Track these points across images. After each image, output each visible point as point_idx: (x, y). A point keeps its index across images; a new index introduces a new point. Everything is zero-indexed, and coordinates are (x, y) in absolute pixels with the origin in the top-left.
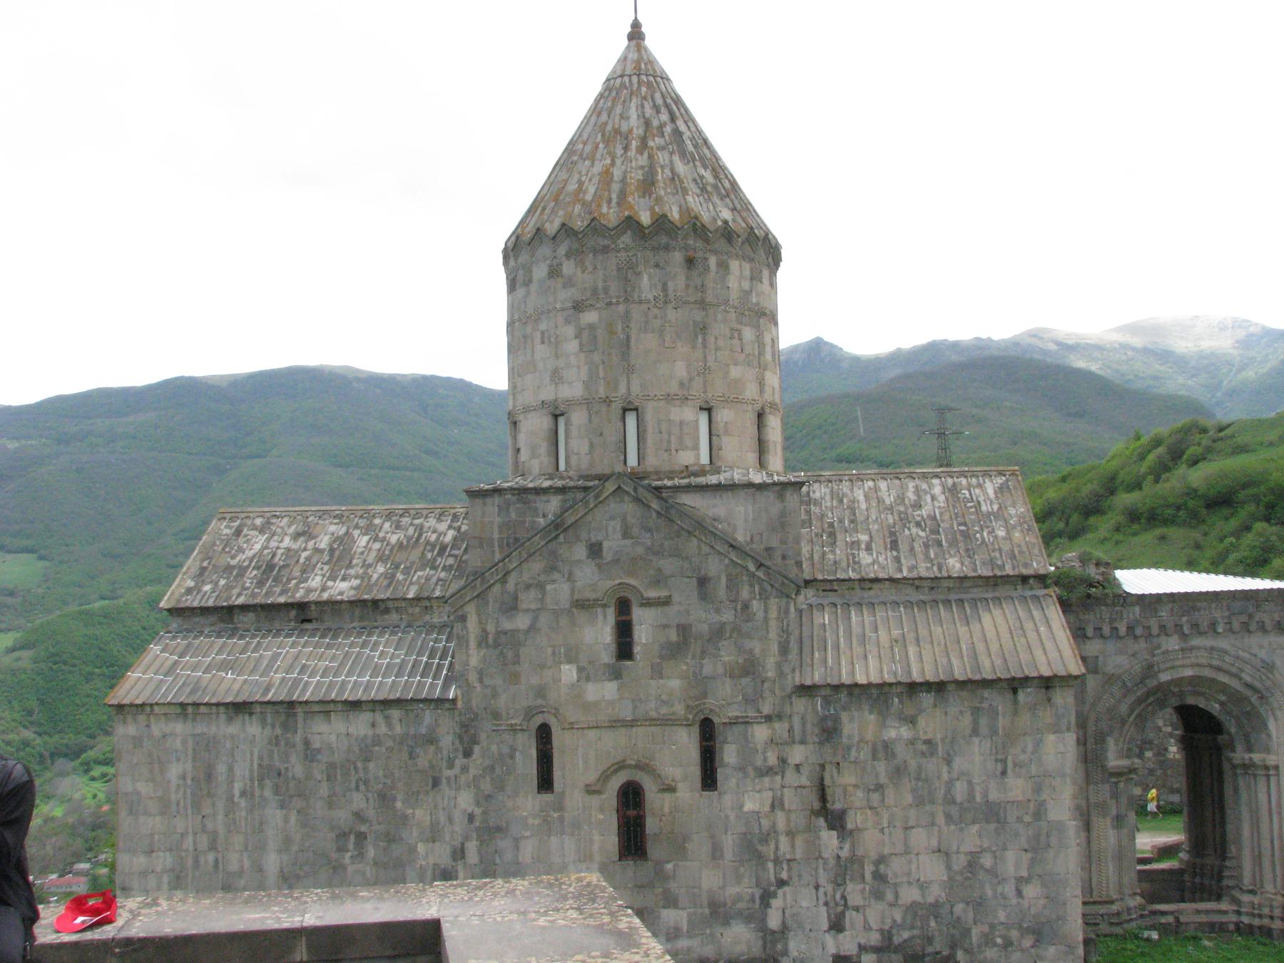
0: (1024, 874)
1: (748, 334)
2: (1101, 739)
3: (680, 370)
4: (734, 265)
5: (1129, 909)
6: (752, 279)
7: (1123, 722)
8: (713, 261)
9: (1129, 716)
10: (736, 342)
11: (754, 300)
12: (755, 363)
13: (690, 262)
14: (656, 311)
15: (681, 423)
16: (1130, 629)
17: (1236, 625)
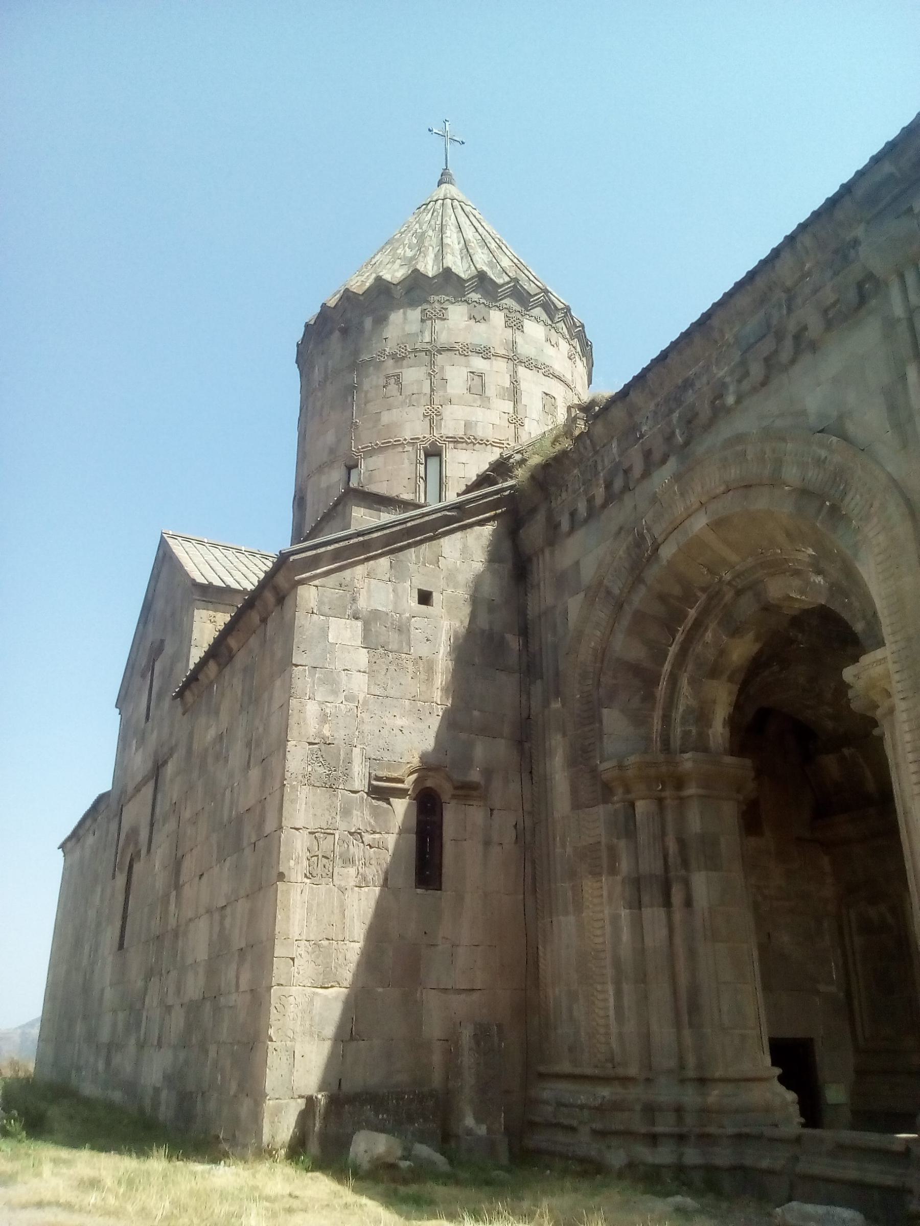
0: (243, 945)
1: (413, 375)
2: (590, 716)
3: (330, 438)
4: (396, 317)
5: (650, 1110)
6: (423, 321)
7: (645, 678)
8: (368, 323)
9: (659, 656)
10: (393, 388)
11: (427, 339)
12: (424, 400)
13: (345, 332)
14: (319, 394)
15: (328, 488)
16: (608, 486)
17: (756, 370)
